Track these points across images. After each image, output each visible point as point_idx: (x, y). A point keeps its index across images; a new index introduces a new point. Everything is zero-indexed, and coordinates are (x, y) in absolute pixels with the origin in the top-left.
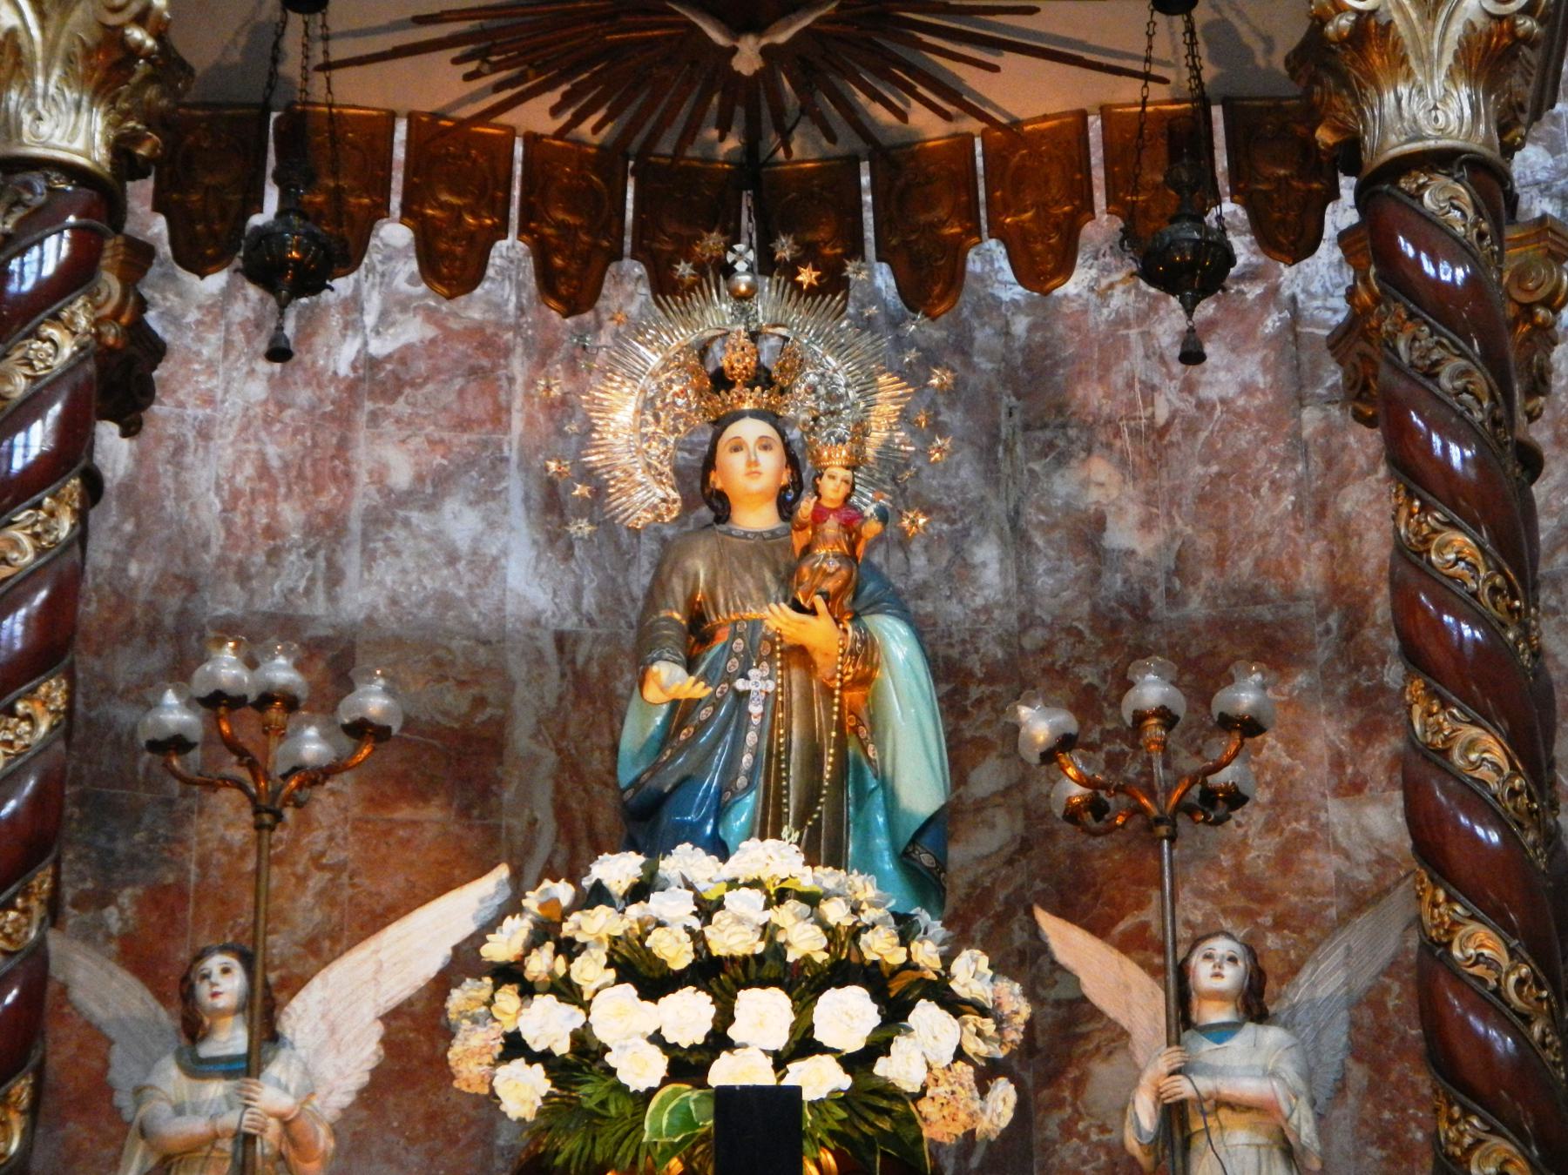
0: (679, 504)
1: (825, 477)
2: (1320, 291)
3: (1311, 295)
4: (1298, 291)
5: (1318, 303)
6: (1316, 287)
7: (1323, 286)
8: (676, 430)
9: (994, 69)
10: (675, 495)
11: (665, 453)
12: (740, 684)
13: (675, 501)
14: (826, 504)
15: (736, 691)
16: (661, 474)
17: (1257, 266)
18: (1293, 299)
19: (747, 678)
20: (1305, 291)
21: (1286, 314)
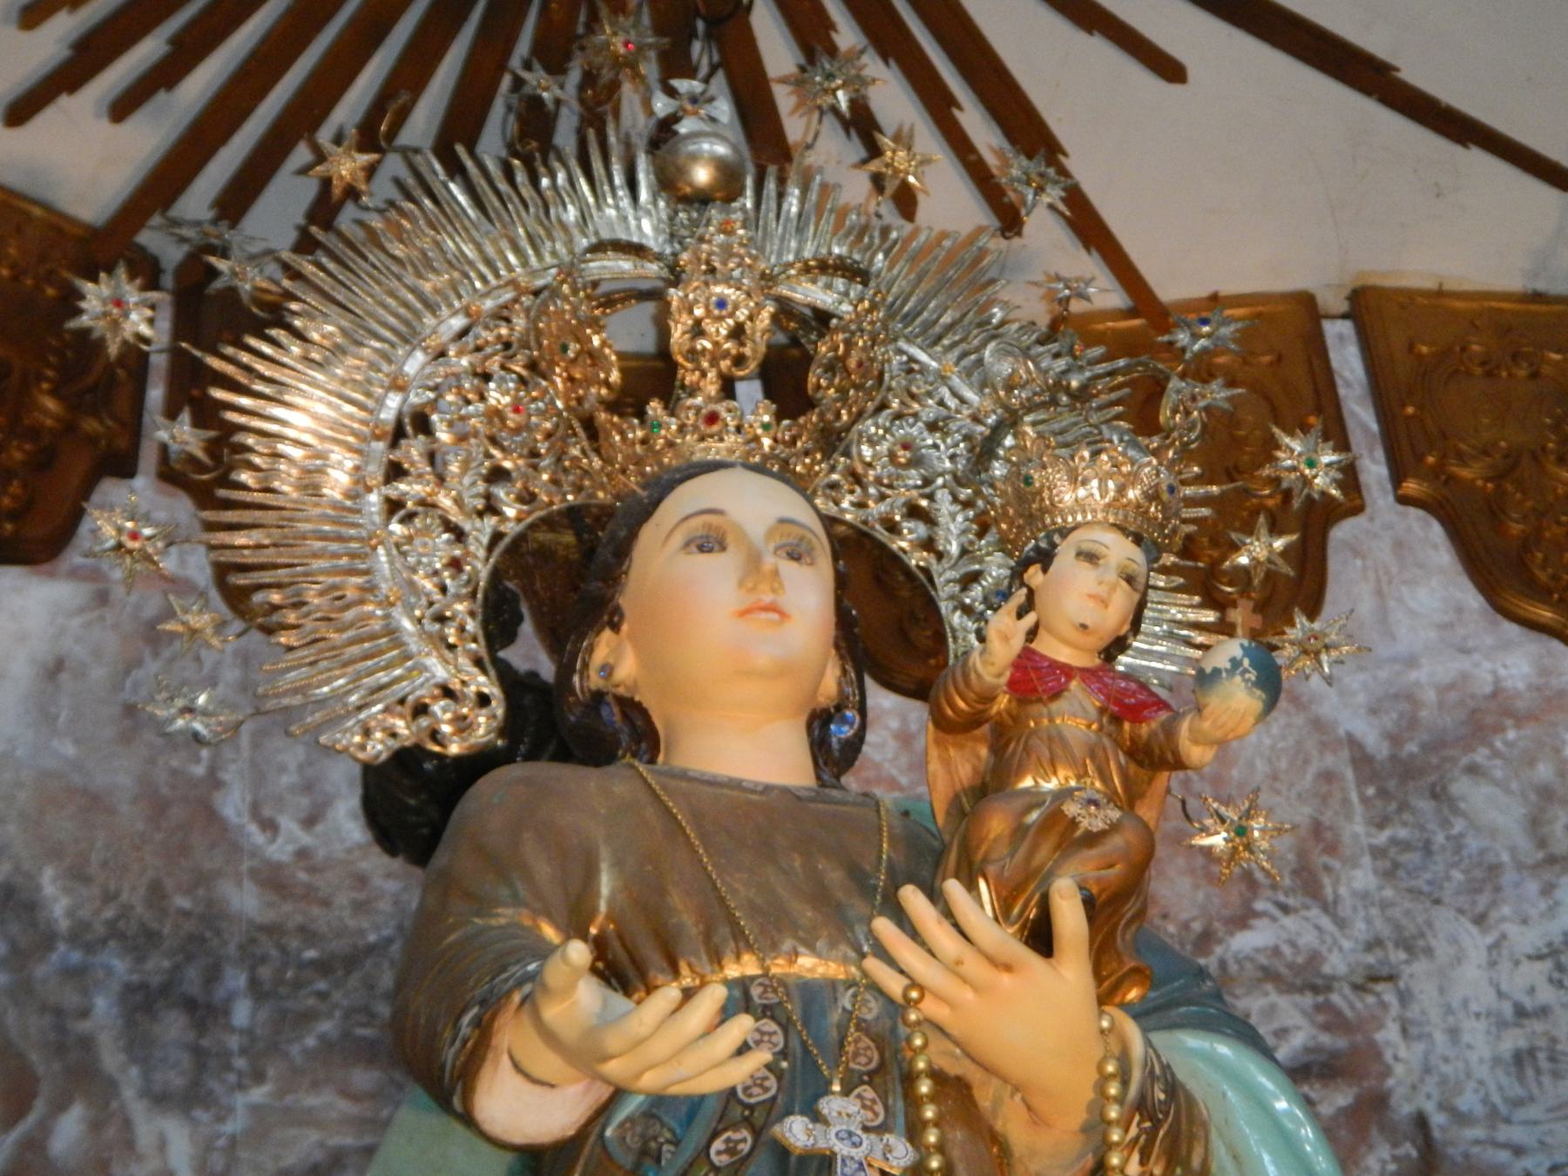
0: (498, 708)
1: (1065, 554)
2: (1479, 1110)
3: (1461, 1118)
4: (1429, 1107)
5: (1478, 1132)
6: (1468, 1101)
7: (1485, 1101)
8: (491, 508)
9: (1170, 70)
10: (483, 683)
11: (455, 565)
12: (796, 1132)
13: (483, 700)
14: (1053, 649)
15: (782, 1152)
16: (441, 619)
17: (1335, 1054)
18: (1421, 1121)
19: (817, 1117)
20: (1444, 1106)
21: (1409, 1150)
